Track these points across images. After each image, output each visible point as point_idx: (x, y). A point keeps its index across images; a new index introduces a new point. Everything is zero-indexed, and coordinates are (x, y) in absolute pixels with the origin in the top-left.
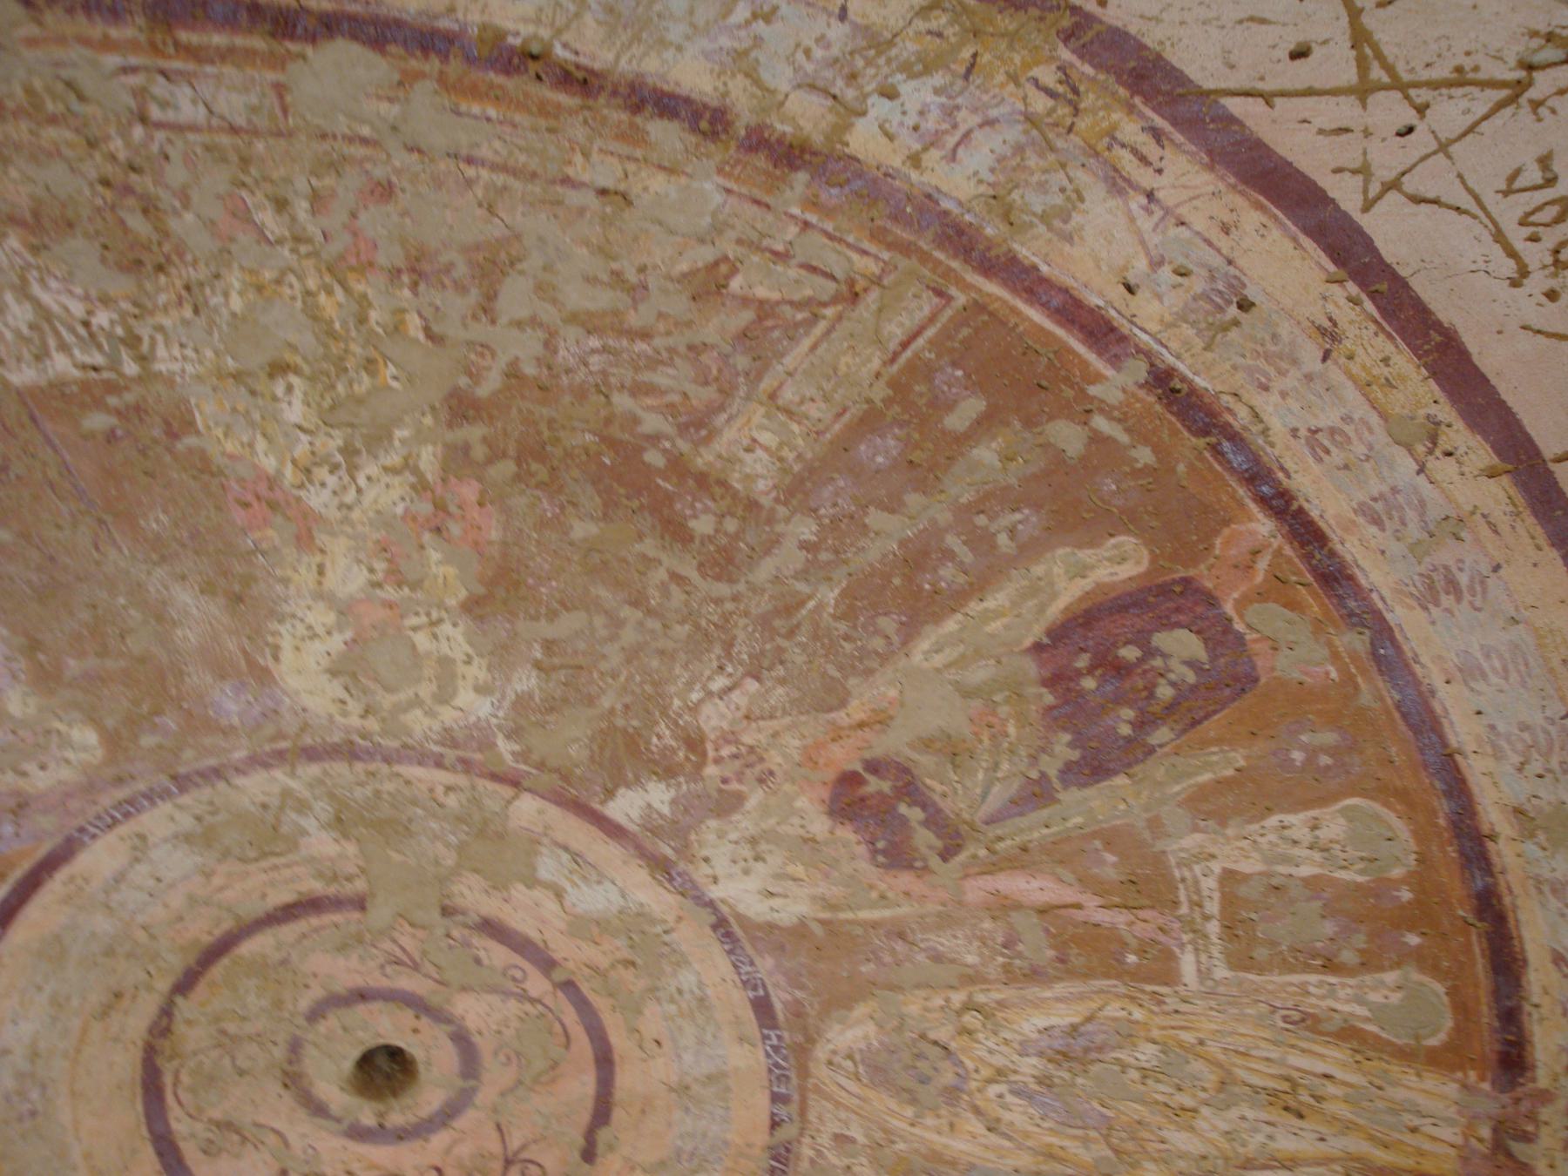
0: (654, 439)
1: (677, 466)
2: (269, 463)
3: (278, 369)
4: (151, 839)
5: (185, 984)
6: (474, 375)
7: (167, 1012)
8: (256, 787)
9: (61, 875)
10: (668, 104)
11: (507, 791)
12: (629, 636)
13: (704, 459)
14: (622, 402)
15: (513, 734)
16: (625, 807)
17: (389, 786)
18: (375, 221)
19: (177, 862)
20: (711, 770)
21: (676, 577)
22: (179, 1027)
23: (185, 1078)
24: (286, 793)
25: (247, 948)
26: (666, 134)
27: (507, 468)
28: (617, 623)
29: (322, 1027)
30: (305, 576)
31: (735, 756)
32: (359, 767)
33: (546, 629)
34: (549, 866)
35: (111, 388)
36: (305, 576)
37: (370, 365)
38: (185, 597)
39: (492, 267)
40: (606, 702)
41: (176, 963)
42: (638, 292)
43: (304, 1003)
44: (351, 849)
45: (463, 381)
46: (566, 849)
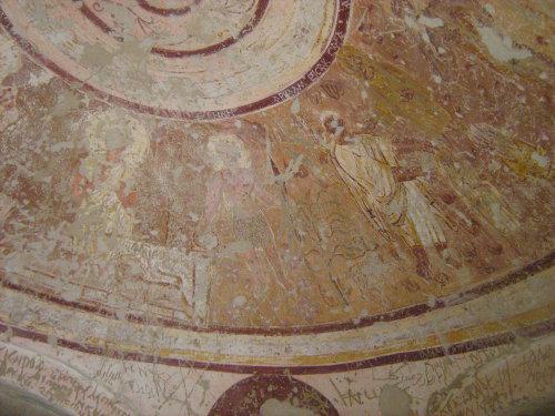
0: (25, 208)
1: (21, 202)
2: (122, 210)
3: (109, 235)
4: (212, 100)
5: (230, 42)
6: (65, 226)
7: (241, 35)
8: (173, 105)
9: (246, 103)
10: (13, 287)
11: (90, 82)
12: (39, 143)
13: (14, 203)
14: (32, 219)
15: (82, 106)
16: (47, 76)
17: (130, 92)
18: (75, 265)
19: (210, 89)
20: (15, 93)
21: (23, 164)
22: (241, 26)
23: (248, 5)
24: (165, 99)
25: (203, 46)
26: (15, 281)
27: (64, 200)
28: (43, 148)
29: (185, 4)
30: (127, 176)
31: (7, 100)
32: (137, 102)
33: (64, 145)
34: (79, 50)
35: (146, 240)
36: (127, 176)
37: (88, 233)
38: (161, 179)
39: (55, 255)
40: (49, 118)
41: (229, 51)
42: (24, 247)
43: (188, 17)
44: (149, 72)
45: (69, 225)
46: (71, 58)
